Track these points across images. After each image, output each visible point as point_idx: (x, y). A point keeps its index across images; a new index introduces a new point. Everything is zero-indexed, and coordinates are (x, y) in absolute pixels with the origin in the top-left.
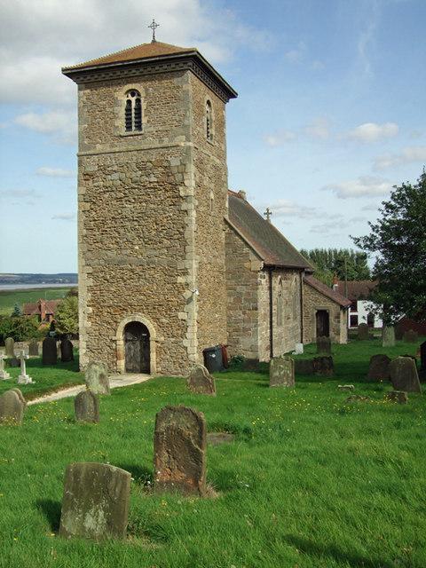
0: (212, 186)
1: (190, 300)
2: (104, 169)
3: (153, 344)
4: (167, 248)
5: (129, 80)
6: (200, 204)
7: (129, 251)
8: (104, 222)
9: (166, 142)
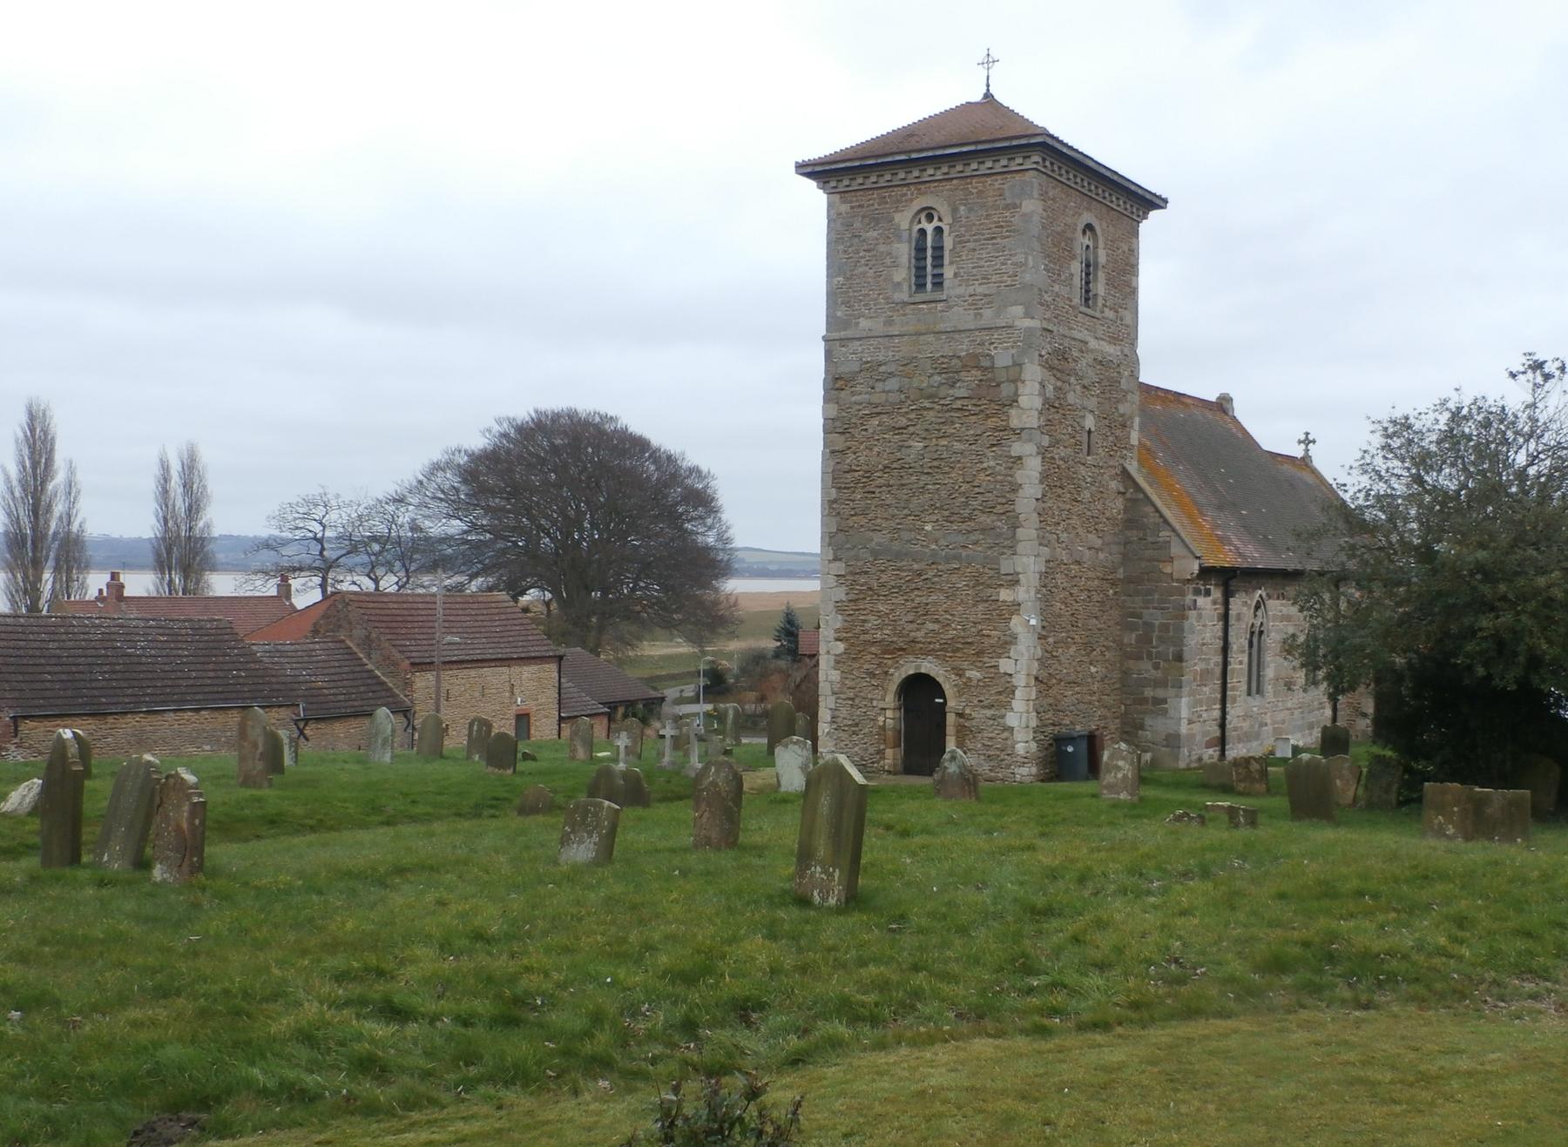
0: (1092, 403)
2: (872, 370)
3: (951, 719)
6: (1055, 443)
8: (868, 474)
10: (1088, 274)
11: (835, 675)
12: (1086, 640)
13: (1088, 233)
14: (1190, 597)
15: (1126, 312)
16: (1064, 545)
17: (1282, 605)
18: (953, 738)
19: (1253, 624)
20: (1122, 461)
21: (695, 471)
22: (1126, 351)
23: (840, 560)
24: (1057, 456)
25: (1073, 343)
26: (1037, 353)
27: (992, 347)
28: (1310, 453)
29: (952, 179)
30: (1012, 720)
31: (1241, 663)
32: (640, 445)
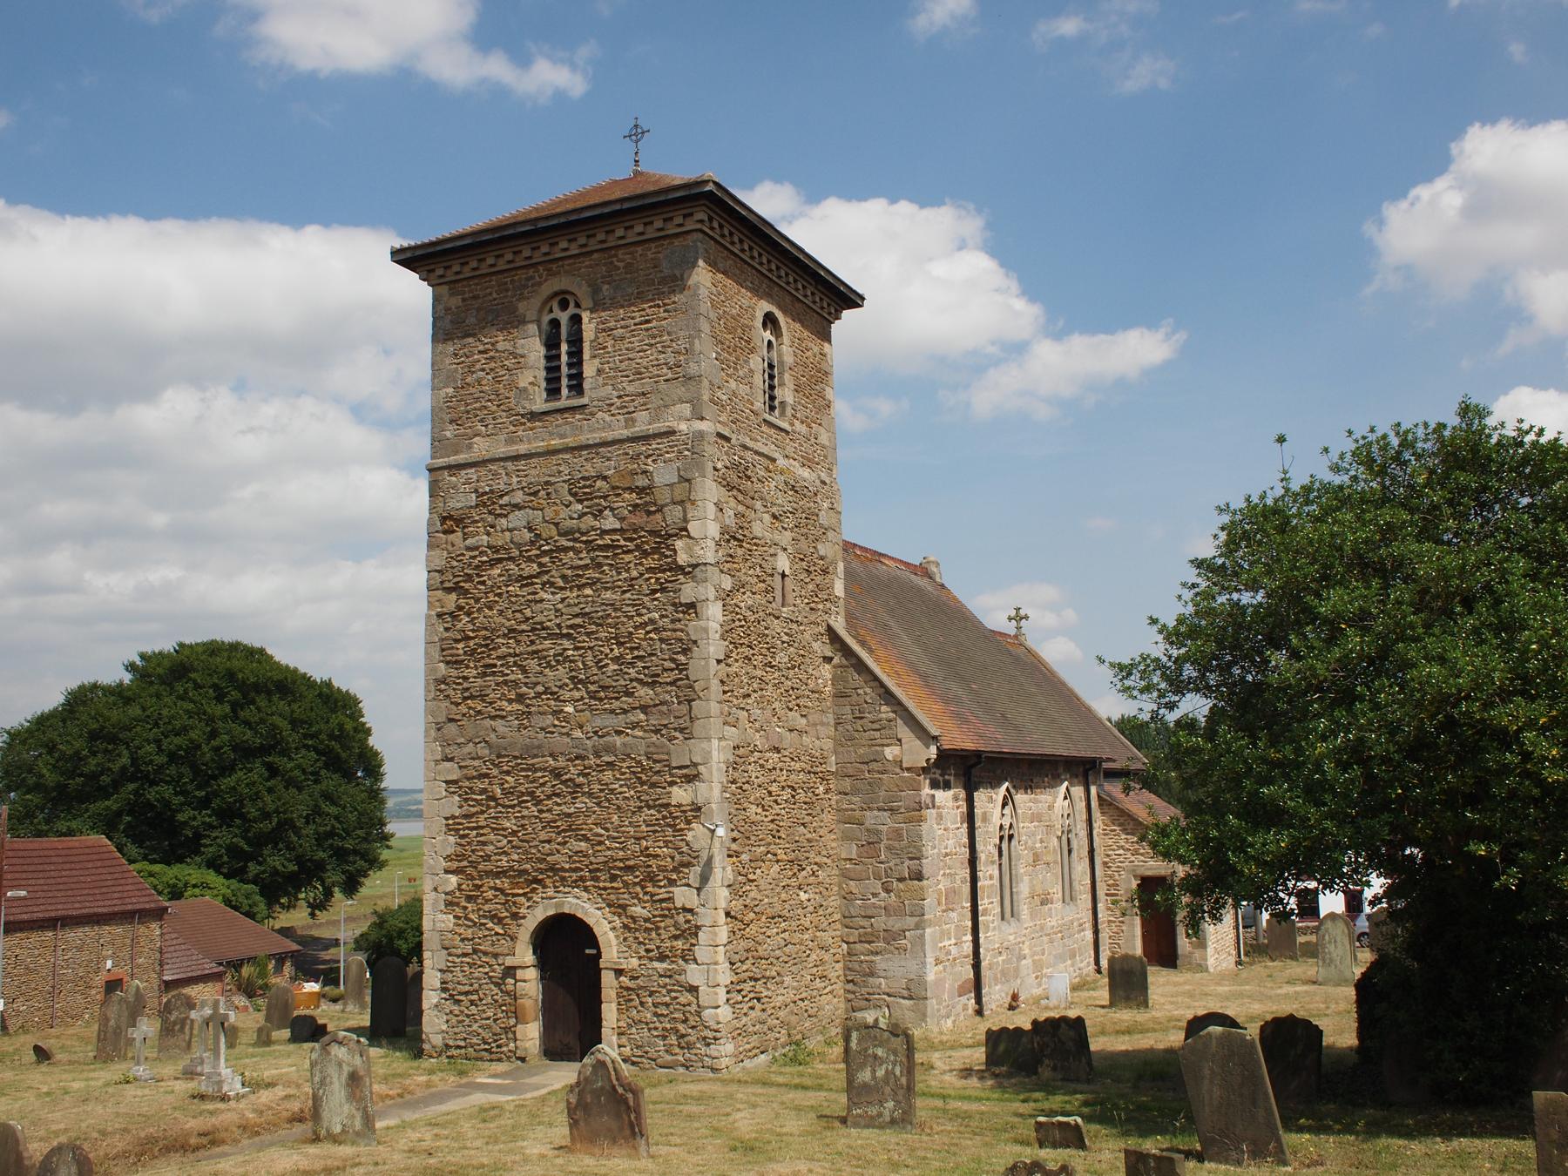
0: (786, 538)
2: (489, 501)
3: (607, 978)
4: (644, 709)
5: (552, 265)
7: (550, 719)
9: (643, 424)
10: (771, 377)
11: (448, 921)
12: (792, 856)
13: (769, 325)
14: (927, 790)
15: (822, 430)
16: (757, 725)
17: (1030, 801)
18: (614, 1006)
19: (1001, 826)
20: (826, 617)
21: (360, 711)
22: (824, 476)
23: (451, 760)
24: (742, 605)
25: (757, 457)
26: (710, 464)
27: (649, 461)
28: (1023, 631)
29: (592, 252)
31: (991, 878)
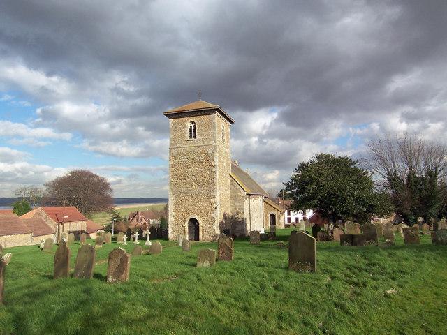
1: (216, 207)
2: (180, 154)
3: (201, 228)
30: (214, 227)
32: (92, 175)
